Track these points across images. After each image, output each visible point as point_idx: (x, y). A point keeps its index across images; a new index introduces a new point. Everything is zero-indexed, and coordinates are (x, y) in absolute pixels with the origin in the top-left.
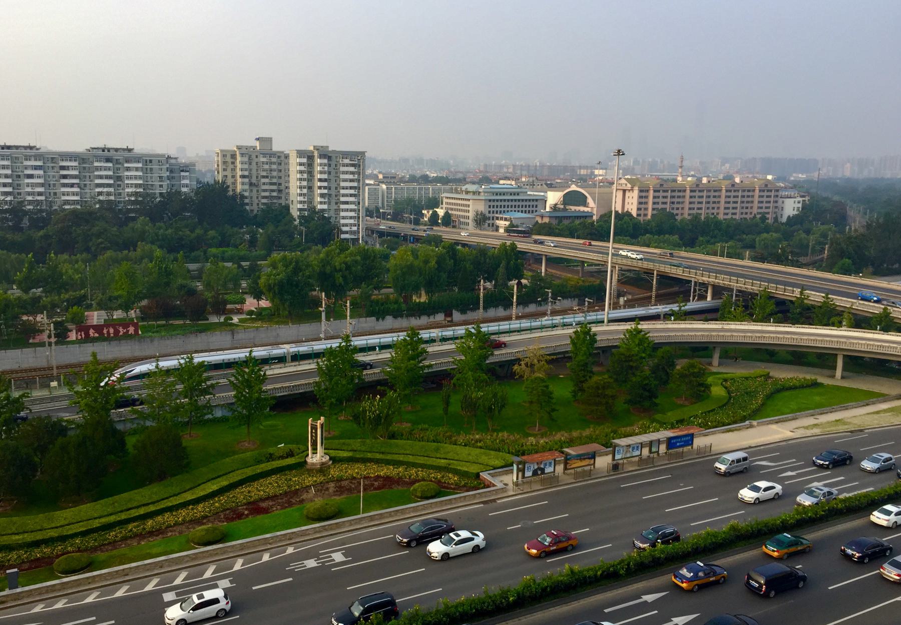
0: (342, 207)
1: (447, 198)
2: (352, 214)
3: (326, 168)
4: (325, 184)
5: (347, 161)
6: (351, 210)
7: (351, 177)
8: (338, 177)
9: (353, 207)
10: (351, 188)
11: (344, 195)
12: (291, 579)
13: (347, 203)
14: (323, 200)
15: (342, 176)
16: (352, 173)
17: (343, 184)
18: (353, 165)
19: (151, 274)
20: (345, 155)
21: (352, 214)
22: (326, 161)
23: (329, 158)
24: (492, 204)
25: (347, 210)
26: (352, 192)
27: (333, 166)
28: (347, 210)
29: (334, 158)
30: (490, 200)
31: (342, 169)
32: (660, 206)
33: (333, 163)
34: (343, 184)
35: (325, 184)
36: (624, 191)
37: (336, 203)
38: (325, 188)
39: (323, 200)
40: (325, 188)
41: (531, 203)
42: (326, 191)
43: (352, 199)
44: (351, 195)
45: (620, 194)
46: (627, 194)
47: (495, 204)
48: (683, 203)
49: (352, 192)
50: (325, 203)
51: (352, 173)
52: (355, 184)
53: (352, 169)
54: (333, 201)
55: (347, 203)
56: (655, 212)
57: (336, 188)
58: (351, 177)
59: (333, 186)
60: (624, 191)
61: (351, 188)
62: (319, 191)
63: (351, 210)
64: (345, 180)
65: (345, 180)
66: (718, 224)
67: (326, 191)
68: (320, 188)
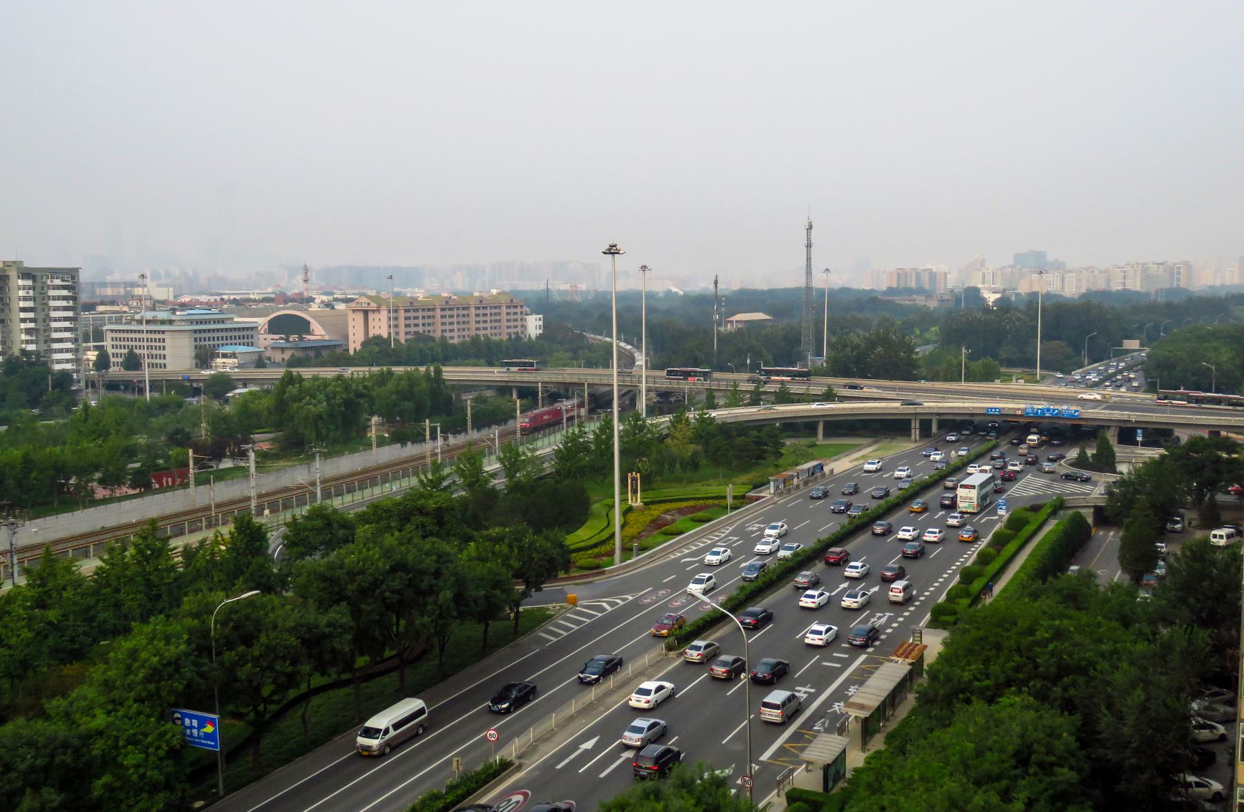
0: (56, 346)
1: (112, 331)
2: (69, 356)
3: (31, 292)
4: (31, 315)
5: (58, 282)
6: (68, 351)
7: (64, 303)
8: (46, 304)
9: (69, 345)
10: (66, 319)
11: (57, 330)
12: (602, 776)
13: (61, 340)
14: (28, 338)
15: (52, 303)
16: (65, 298)
17: (54, 314)
18: (64, 287)
19: (105, 434)
20: (55, 272)
21: (69, 356)
22: (30, 283)
23: (34, 278)
24: (198, 335)
25: (61, 351)
26: (67, 324)
27: (38, 290)
28: (61, 351)
29: (39, 279)
30: (195, 331)
31: (52, 293)
32: (413, 329)
33: (39, 285)
34: (54, 314)
35: (31, 315)
36: (366, 313)
37: (46, 342)
38: (31, 320)
39: (28, 338)
40: (31, 320)
41: (246, 333)
42: (32, 325)
43: (68, 335)
44: (66, 330)
45: (360, 317)
46: (371, 316)
47: (203, 335)
48: (508, 314)
49: (67, 324)
50: (32, 342)
51: (65, 298)
52: (70, 314)
53: (65, 293)
54: (42, 338)
55: (61, 340)
56: (409, 337)
57: (44, 321)
58: (64, 303)
59: (41, 316)
60: (366, 313)
61: (66, 319)
62: (23, 326)
63: (68, 351)
64: (57, 309)
65: (57, 309)
66: (498, 344)
67: (32, 325)
68: (24, 320)
